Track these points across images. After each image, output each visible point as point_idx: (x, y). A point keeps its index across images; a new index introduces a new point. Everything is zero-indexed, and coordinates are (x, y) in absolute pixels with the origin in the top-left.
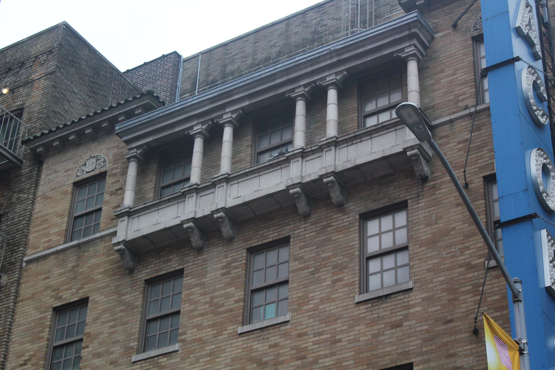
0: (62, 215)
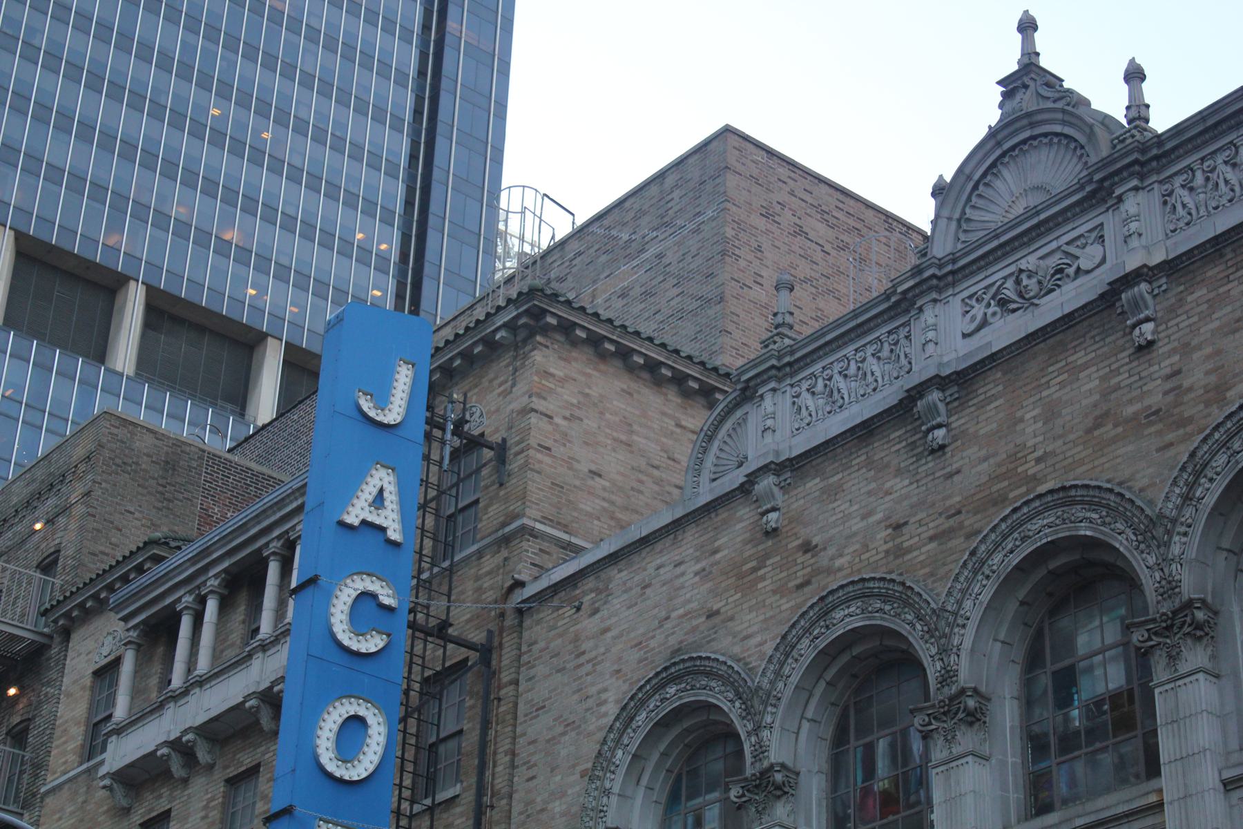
0: (79, 723)
